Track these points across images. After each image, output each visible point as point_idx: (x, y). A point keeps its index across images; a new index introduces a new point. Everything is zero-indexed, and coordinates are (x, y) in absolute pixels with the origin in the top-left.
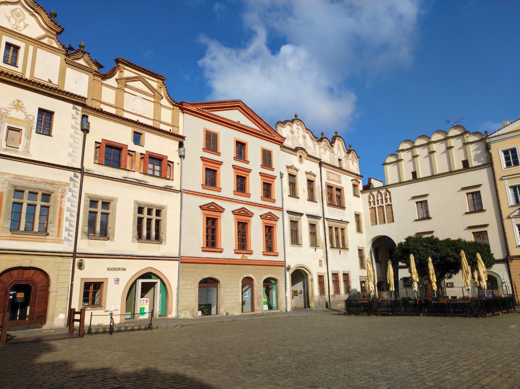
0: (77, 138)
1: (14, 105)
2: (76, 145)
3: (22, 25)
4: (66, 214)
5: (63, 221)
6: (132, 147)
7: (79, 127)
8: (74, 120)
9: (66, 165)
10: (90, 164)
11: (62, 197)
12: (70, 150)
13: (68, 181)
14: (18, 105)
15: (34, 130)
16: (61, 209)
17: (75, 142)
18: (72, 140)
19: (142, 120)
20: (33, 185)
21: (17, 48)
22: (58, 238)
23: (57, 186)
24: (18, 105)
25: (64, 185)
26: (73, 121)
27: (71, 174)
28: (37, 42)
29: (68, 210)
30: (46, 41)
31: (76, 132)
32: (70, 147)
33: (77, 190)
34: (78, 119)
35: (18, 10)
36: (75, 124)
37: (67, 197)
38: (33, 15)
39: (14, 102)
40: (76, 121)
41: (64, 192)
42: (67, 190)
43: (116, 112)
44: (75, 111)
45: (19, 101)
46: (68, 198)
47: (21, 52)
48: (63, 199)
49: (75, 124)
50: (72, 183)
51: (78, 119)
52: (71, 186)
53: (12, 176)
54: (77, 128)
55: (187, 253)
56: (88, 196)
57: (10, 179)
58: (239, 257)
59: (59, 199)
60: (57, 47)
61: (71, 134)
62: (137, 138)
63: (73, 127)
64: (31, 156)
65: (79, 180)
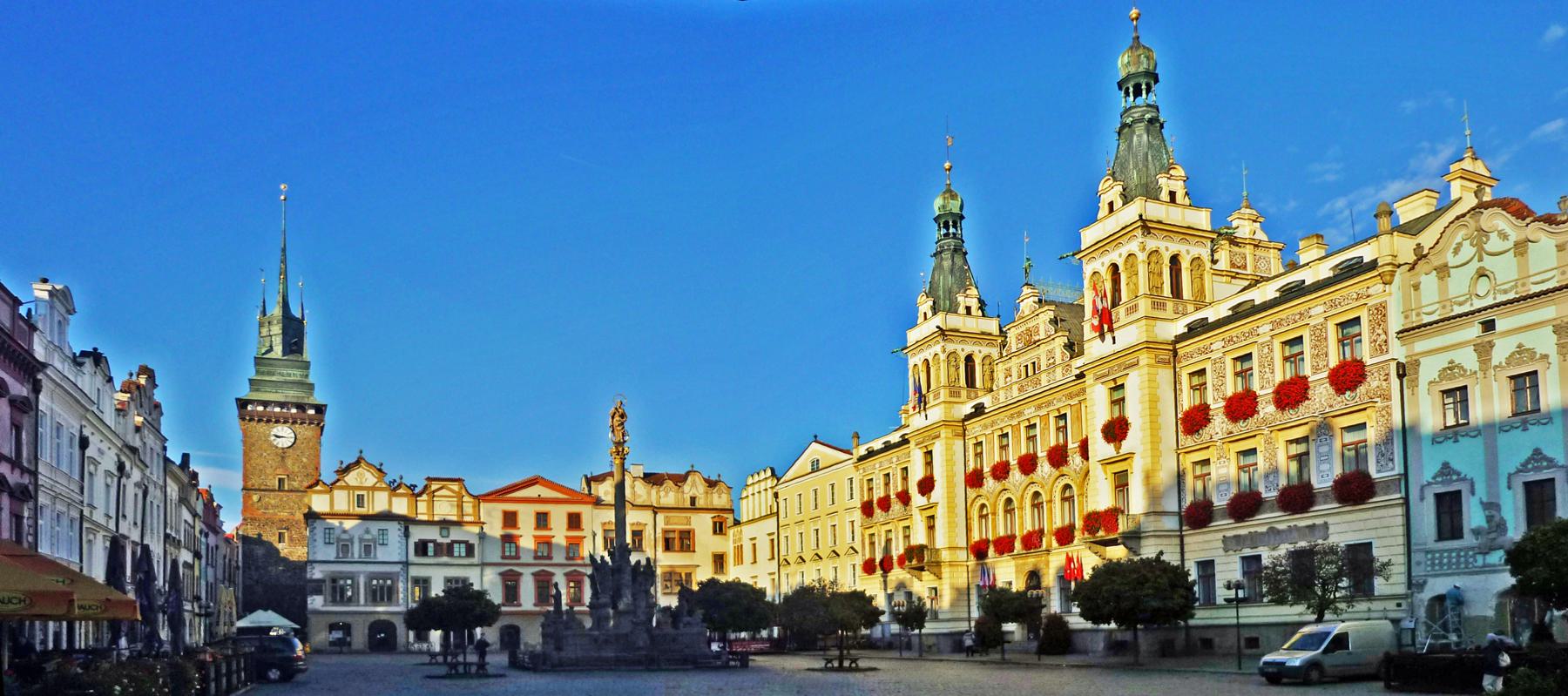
3: (364, 480)
6: (440, 540)
9: (397, 560)
10: (412, 558)
12: (399, 551)
21: (363, 495)
24: (367, 532)
26: (399, 532)
27: (400, 566)
28: (373, 489)
30: (378, 485)
33: (405, 575)
38: (368, 471)
41: (398, 577)
47: (366, 498)
56: (412, 577)
58: (538, 609)
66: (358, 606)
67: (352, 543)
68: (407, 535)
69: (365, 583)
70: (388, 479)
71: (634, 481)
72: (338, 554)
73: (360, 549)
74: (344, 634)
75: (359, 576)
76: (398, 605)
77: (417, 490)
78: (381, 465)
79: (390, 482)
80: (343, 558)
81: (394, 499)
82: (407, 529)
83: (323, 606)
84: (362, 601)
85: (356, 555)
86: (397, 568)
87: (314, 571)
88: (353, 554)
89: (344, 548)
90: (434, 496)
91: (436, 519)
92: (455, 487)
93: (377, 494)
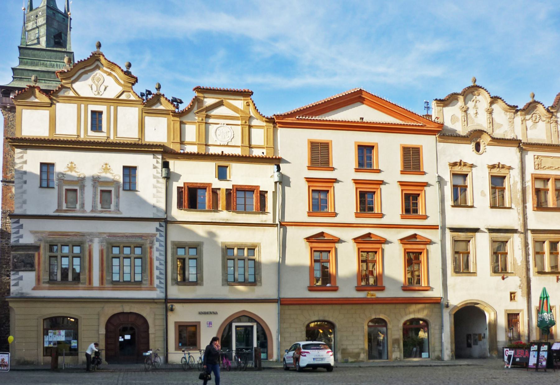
0: (159, 188)
1: (103, 169)
2: (159, 194)
4: (156, 263)
5: (154, 270)
6: (217, 184)
7: (159, 175)
8: (155, 170)
9: (151, 216)
11: (151, 248)
13: (154, 231)
14: (106, 168)
15: (121, 189)
16: (151, 259)
17: (158, 192)
18: (154, 191)
19: (228, 151)
20: (125, 240)
21: (101, 113)
22: (152, 286)
23: (145, 238)
24: (106, 168)
25: (152, 236)
27: (157, 224)
29: (158, 259)
30: (123, 97)
31: (158, 182)
32: (154, 197)
33: (163, 239)
34: (158, 168)
35: (98, 75)
36: (157, 173)
37: (155, 247)
39: (103, 166)
40: (157, 170)
41: (152, 243)
42: (155, 241)
43: (198, 149)
44: (155, 160)
45: (106, 164)
46: (157, 248)
47: (104, 117)
48: (152, 250)
49: (157, 173)
50: (158, 233)
51: (158, 168)
52: (158, 236)
53: (108, 235)
54: (158, 178)
55: (288, 294)
56: (173, 243)
57: (107, 237)
59: (149, 250)
60: (134, 99)
61: (153, 185)
62: (222, 174)
63: (155, 177)
64: (121, 213)
65: (163, 229)
66: (91, 288)
67: (83, 187)
68: (169, 177)
69: (102, 252)
70: (139, 88)
71: (492, 103)
72: (60, 204)
73: (94, 197)
74: (67, 335)
75: (91, 241)
76: (152, 289)
77: (182, 107)
78: (129, 65)
79: (142, 95)
80: (65, 211)
81: (149, 120)
82: (166, 165)
83: (34, 289)
84: (96, 282)
85: (88, 208)
86: (151, 228)
87: (21, 232)
88: (83, 205)
89: (70, 195)
90: (208, 117)
91: (213, 150)
92: (239, 103)
93: (121, 110)
